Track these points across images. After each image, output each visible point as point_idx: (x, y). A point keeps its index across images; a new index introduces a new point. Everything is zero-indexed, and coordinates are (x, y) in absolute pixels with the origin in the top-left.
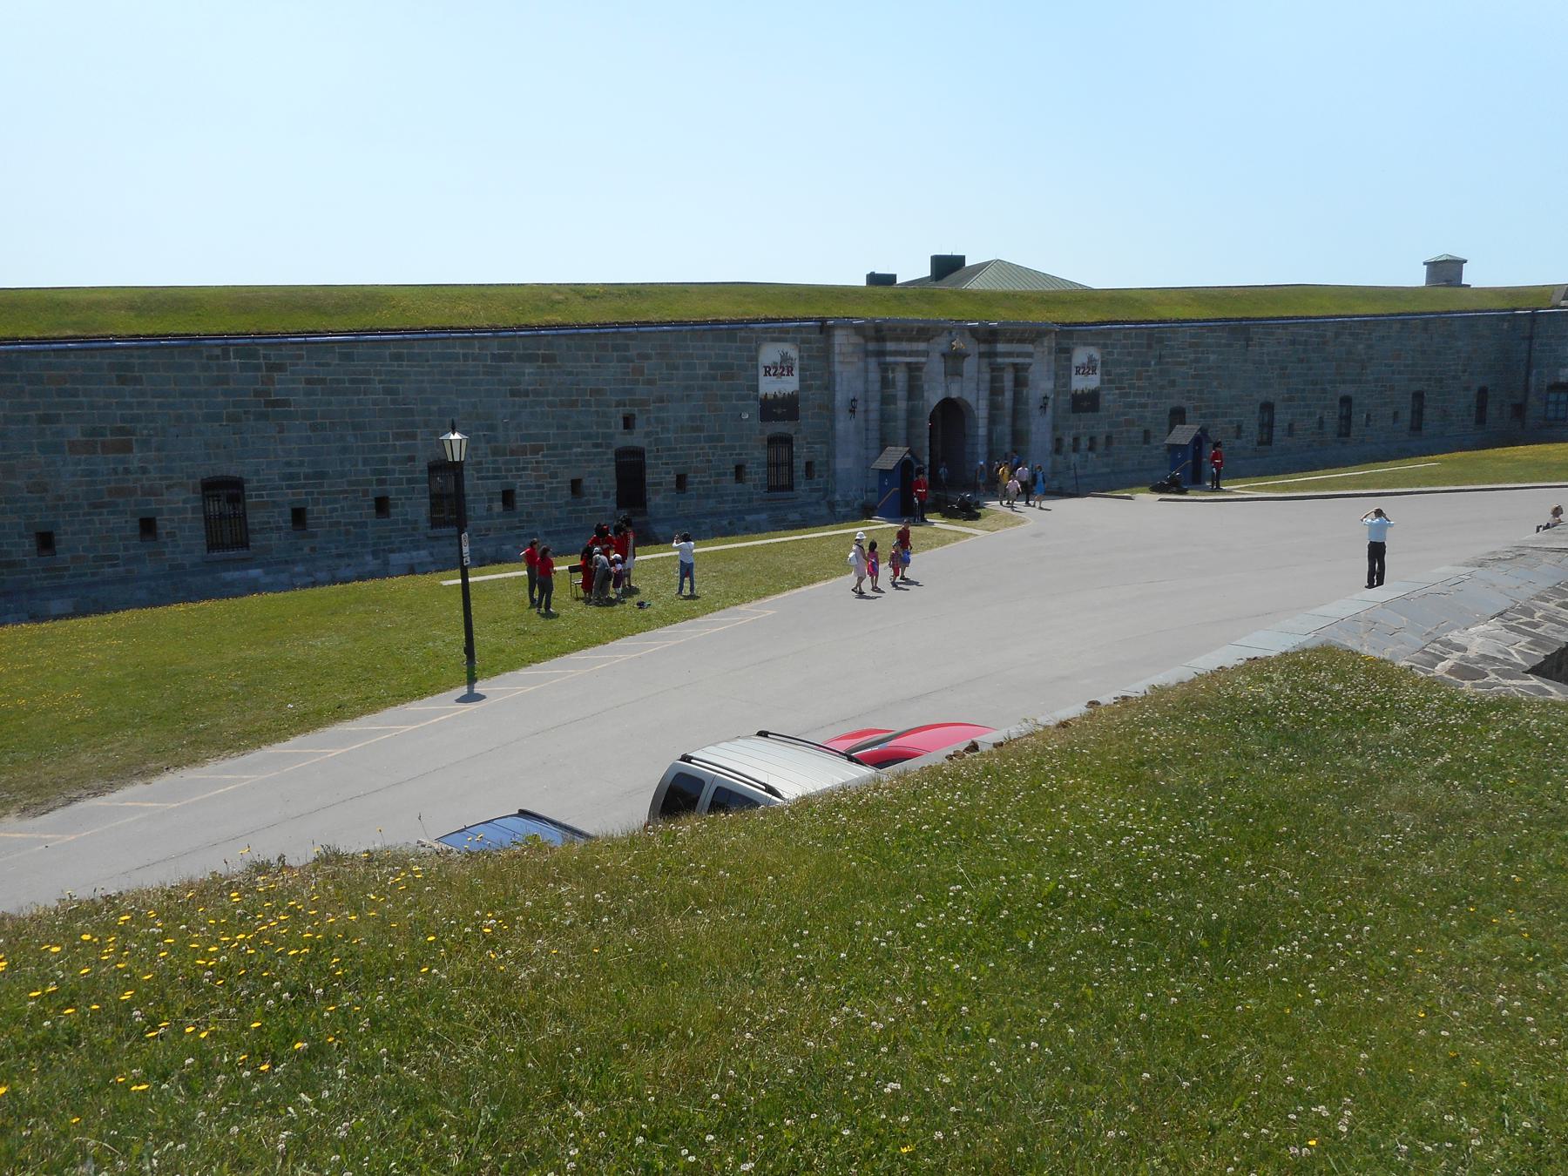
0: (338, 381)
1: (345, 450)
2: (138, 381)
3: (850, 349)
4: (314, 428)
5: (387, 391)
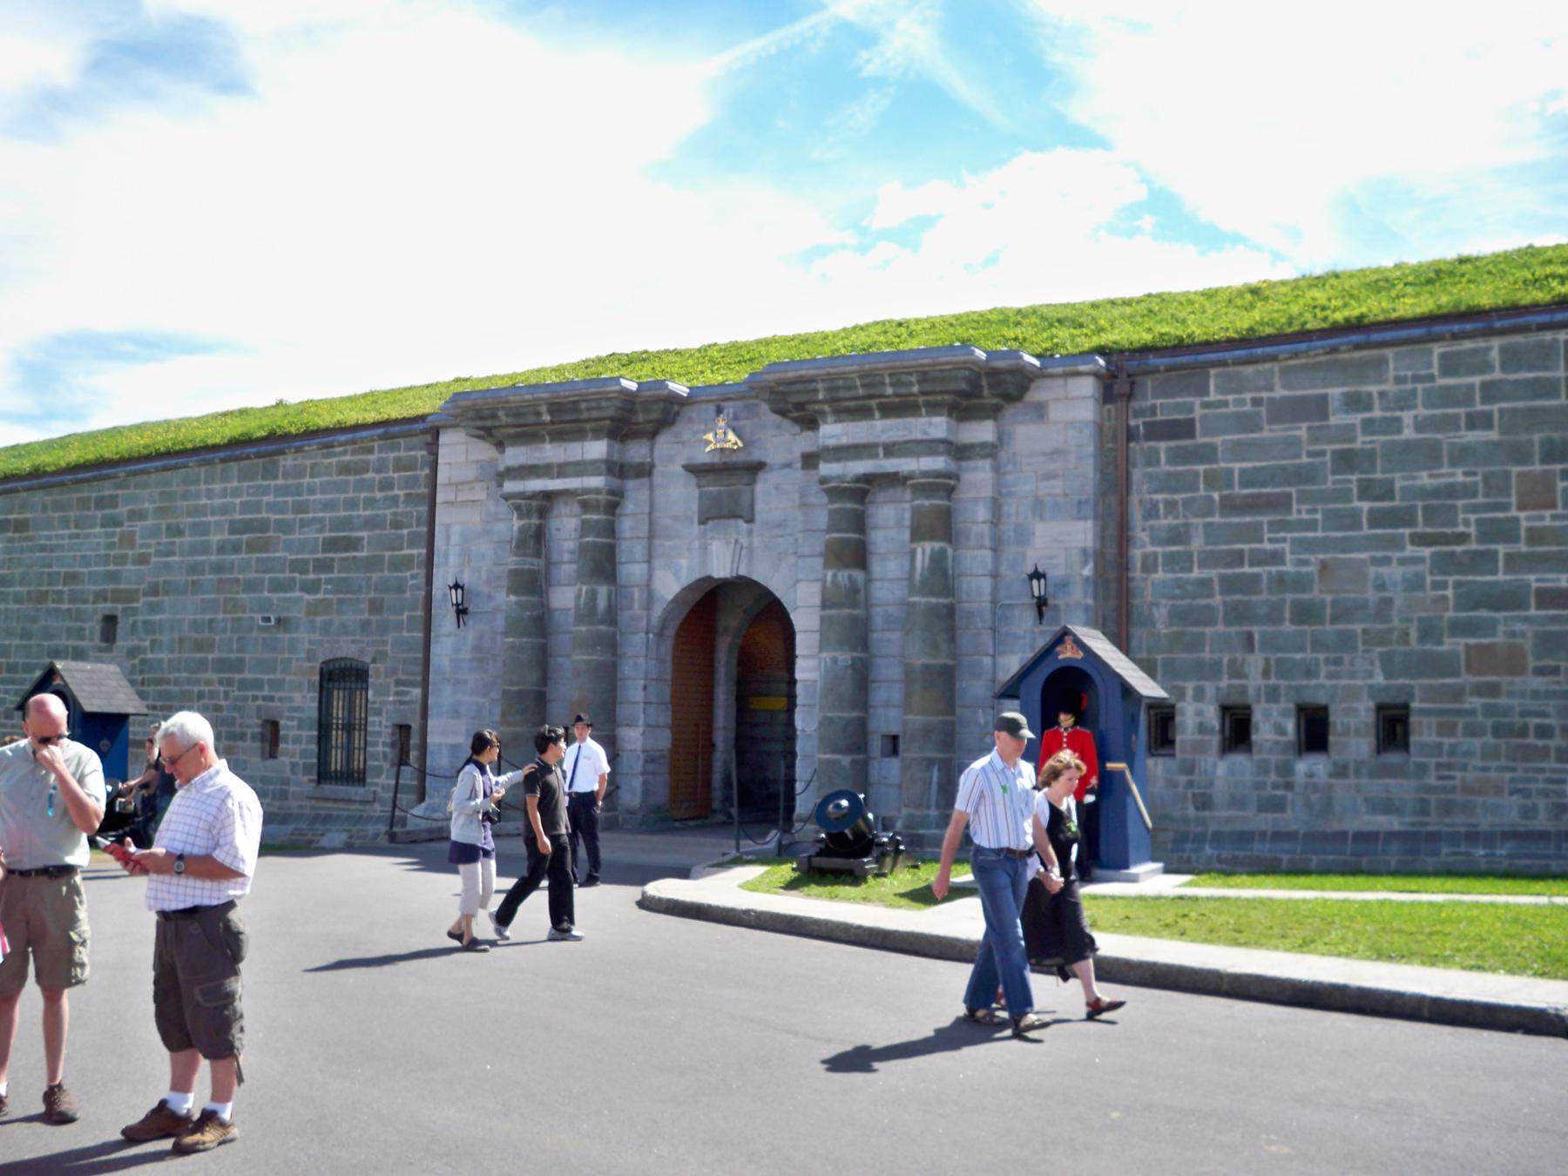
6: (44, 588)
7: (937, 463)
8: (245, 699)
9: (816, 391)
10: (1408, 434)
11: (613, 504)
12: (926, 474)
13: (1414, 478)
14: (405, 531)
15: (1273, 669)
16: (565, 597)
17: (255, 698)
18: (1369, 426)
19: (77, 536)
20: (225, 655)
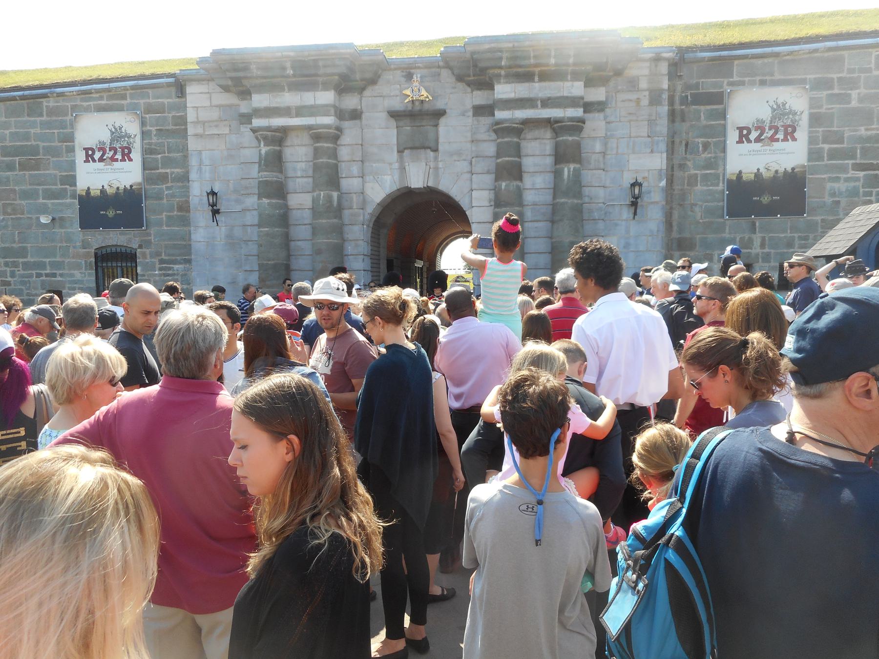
3: (215, 114)
7: (578, 112)
8: (31, 276)
9: (501, 58)
10: (854, 104)
11: (335, 137)
12: (571, 119)
13: (856, 131)
14: (159, 156)
15: (767, 242)
16: (301, 200)
17: (39, 275)
18: (832, 98)
20: (7, 245)
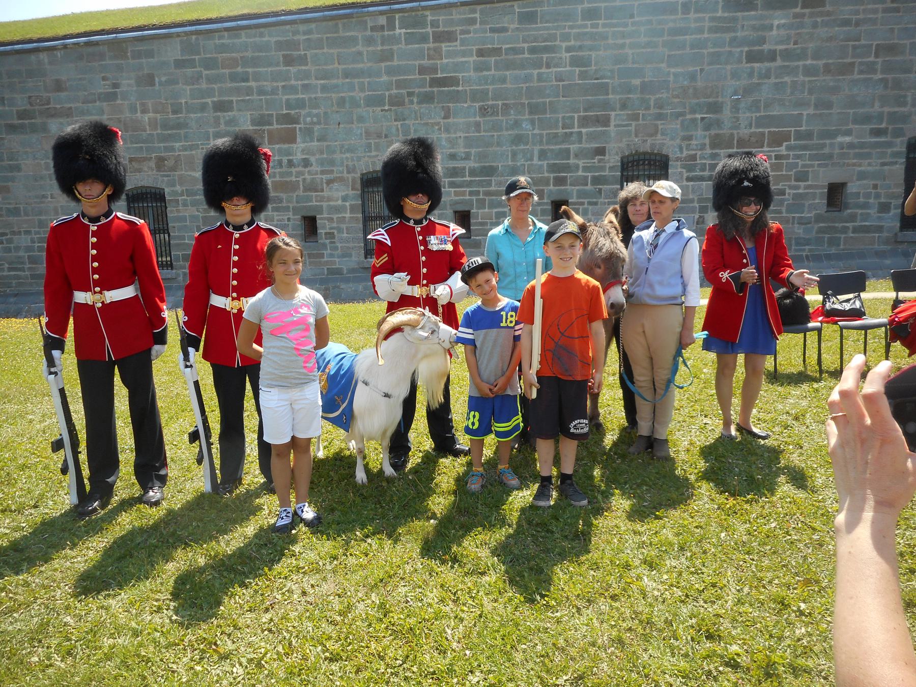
0: (515, 51)
1: (519, 139)
2: (303, 60)
4: (484, 111)
5: (576, 62)
6: (849, 60)
19: (897, 10)
